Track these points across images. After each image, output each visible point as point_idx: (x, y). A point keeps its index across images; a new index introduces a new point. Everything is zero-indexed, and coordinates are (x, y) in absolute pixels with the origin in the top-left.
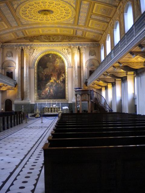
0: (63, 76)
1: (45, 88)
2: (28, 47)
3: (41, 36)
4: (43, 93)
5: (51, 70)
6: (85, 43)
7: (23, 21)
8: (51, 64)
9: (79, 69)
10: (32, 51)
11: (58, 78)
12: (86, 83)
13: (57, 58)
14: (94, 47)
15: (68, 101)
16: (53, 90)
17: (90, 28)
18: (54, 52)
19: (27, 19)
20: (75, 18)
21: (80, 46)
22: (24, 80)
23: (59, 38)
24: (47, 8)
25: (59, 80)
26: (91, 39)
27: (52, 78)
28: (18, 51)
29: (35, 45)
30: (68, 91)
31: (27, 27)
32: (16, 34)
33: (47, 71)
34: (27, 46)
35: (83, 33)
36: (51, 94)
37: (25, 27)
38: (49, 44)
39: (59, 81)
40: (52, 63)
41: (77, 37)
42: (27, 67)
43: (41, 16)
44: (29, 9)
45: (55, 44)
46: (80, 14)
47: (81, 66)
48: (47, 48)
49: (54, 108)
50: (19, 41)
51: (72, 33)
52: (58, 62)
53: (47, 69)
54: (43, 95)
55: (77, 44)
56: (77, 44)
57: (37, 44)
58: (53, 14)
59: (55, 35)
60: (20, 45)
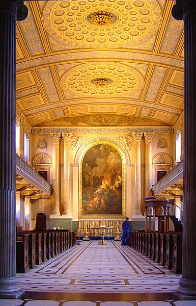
1: (92, 198)
2: (70, 133)
3: (88, 115)
4: (90, 205)
5: (102, 170)
7: (67, 94)
8: (103, 160)
10: (75, 139)
11: (112, 183)
13: (111, 151)
16: (105, 200)
17: (163, 105)
19: (74, 91)
20: (142, 91)
24: (104, 76)
28: (55, 140)
31: (71, 103)
32: (54, 112)
33: (96, 172)
35: (151, 111)
37: (68, 103)
38: (100, 129)
40: (104, 158)
42: (67, 164)
43: (94, 87)
44: (80, 77)
46: (151, 85)
47: (147, 164)
48: (94, 135)
50: (55, 123)
52: (112, 158)
53: (96, 167)
54: (90, 207)
56: (141, 129)
58: (112, 85)
59: (108, 115)
60: (58, 131)
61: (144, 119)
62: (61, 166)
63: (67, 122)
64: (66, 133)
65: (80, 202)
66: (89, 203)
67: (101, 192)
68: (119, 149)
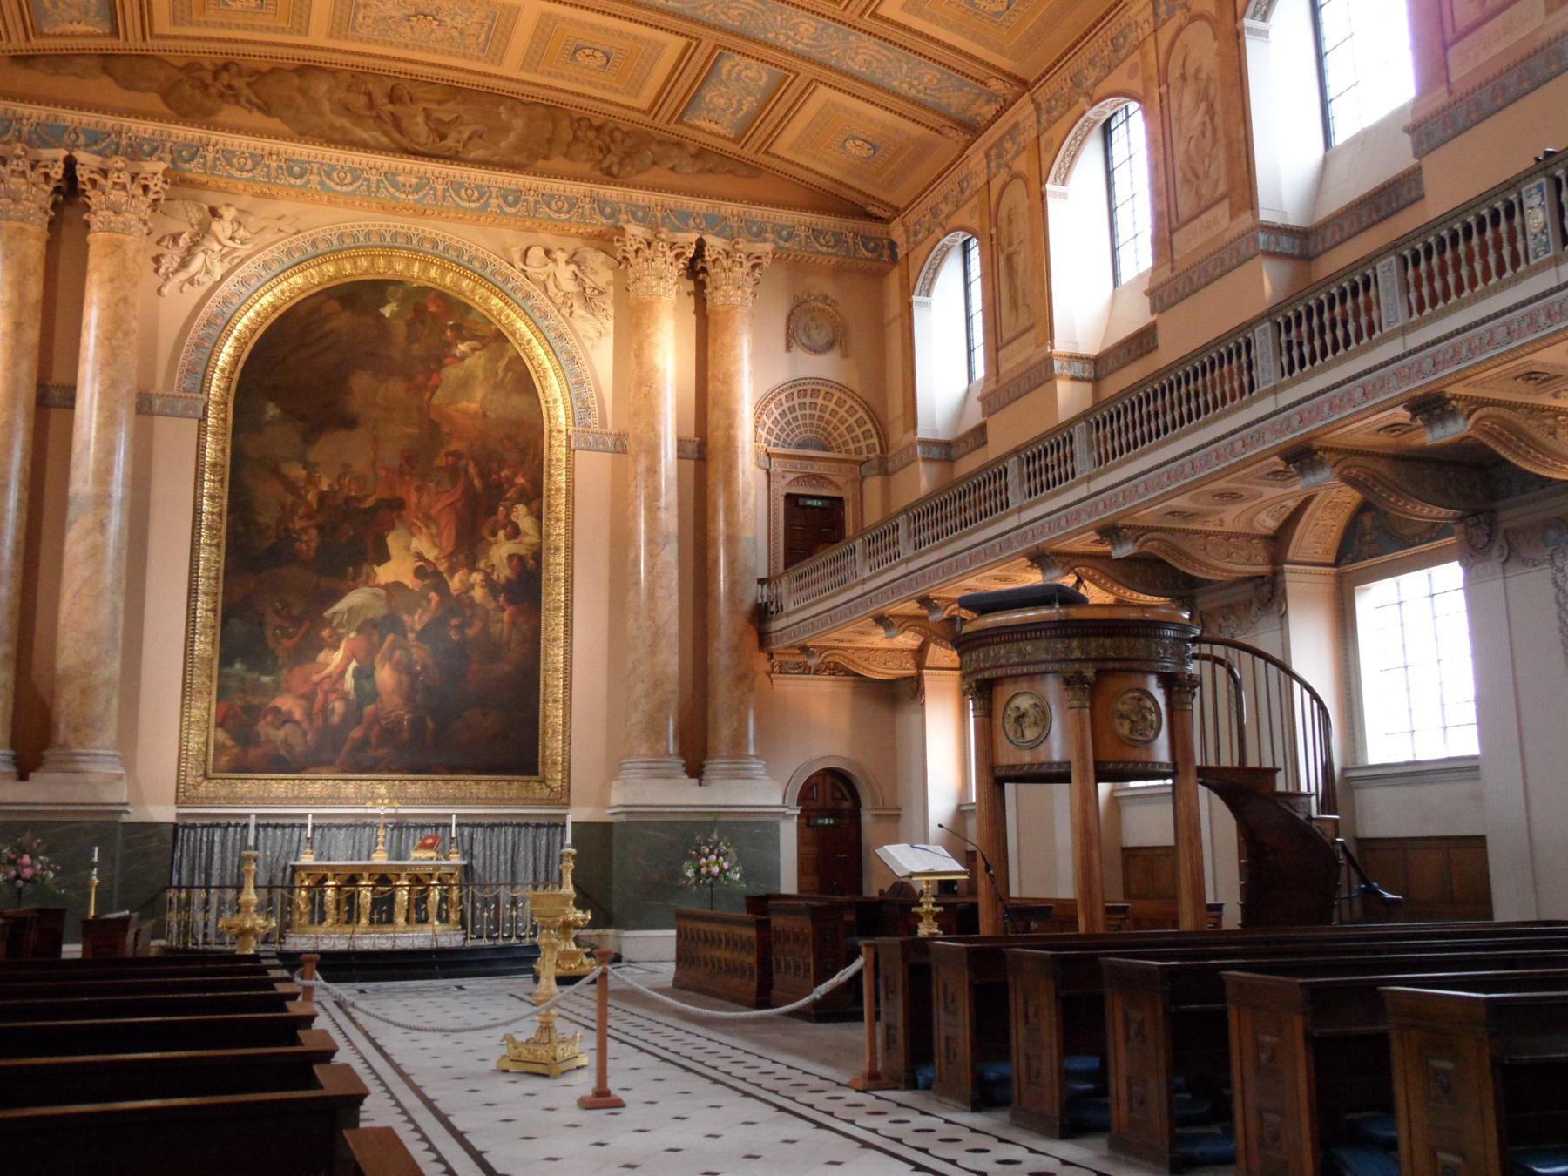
0: (515, 533)
1: (309, 649)
3: (304, 70)
4: (286, 703)
5: (391, 456)
6: (758, 213)
8: (397, 387)
9: (692, 463)
10: (184, 220)
12: (761, 615)
13: (461, 332)
14: (837, 272)
15: (563, 798)
16: (405, 668)
18: (433, 273)
21: (715, 243)
22: (72, 535)
23: (506, 130)
25: (473, 568)
26: (813, 189)
27: (393, 541)
29: (228, 155)
30: (568, 687)
34: (136, 152)
36: (376, 718)
38: (390, 176)
39: (477, 577)
41: (679, 145)
45: (457, 186)
49: (416, 880)
51: (644, 101)
52: (465, 384)
53: (342, 434)
54: (285, 719)
55: (682, 219)
57: (257, 159)
59: (455, 92)
60: (49, 135)
61: (701, 153)
62: (56, 395)
63: (129, 86)
64: (118, 162)
65: (199, 680)
66: (277, 689)
67: (379, 610)
68: (521, 326)
